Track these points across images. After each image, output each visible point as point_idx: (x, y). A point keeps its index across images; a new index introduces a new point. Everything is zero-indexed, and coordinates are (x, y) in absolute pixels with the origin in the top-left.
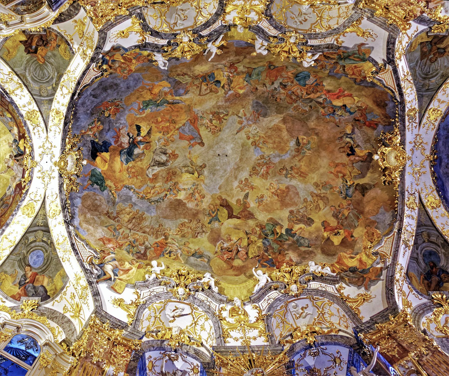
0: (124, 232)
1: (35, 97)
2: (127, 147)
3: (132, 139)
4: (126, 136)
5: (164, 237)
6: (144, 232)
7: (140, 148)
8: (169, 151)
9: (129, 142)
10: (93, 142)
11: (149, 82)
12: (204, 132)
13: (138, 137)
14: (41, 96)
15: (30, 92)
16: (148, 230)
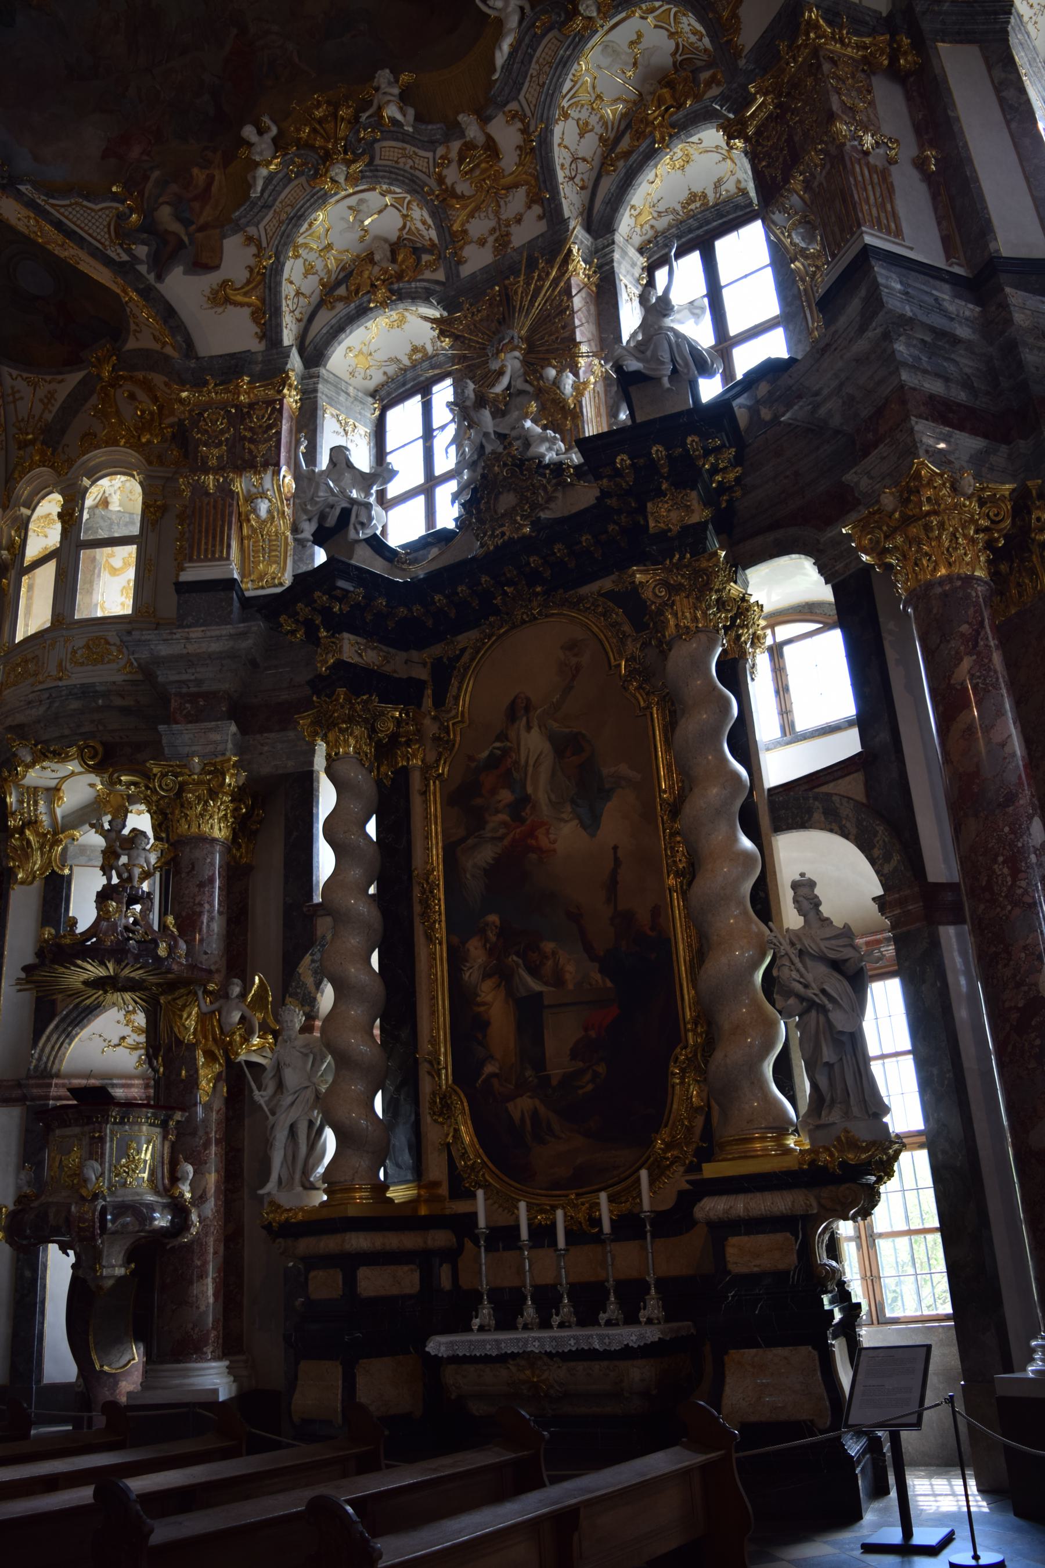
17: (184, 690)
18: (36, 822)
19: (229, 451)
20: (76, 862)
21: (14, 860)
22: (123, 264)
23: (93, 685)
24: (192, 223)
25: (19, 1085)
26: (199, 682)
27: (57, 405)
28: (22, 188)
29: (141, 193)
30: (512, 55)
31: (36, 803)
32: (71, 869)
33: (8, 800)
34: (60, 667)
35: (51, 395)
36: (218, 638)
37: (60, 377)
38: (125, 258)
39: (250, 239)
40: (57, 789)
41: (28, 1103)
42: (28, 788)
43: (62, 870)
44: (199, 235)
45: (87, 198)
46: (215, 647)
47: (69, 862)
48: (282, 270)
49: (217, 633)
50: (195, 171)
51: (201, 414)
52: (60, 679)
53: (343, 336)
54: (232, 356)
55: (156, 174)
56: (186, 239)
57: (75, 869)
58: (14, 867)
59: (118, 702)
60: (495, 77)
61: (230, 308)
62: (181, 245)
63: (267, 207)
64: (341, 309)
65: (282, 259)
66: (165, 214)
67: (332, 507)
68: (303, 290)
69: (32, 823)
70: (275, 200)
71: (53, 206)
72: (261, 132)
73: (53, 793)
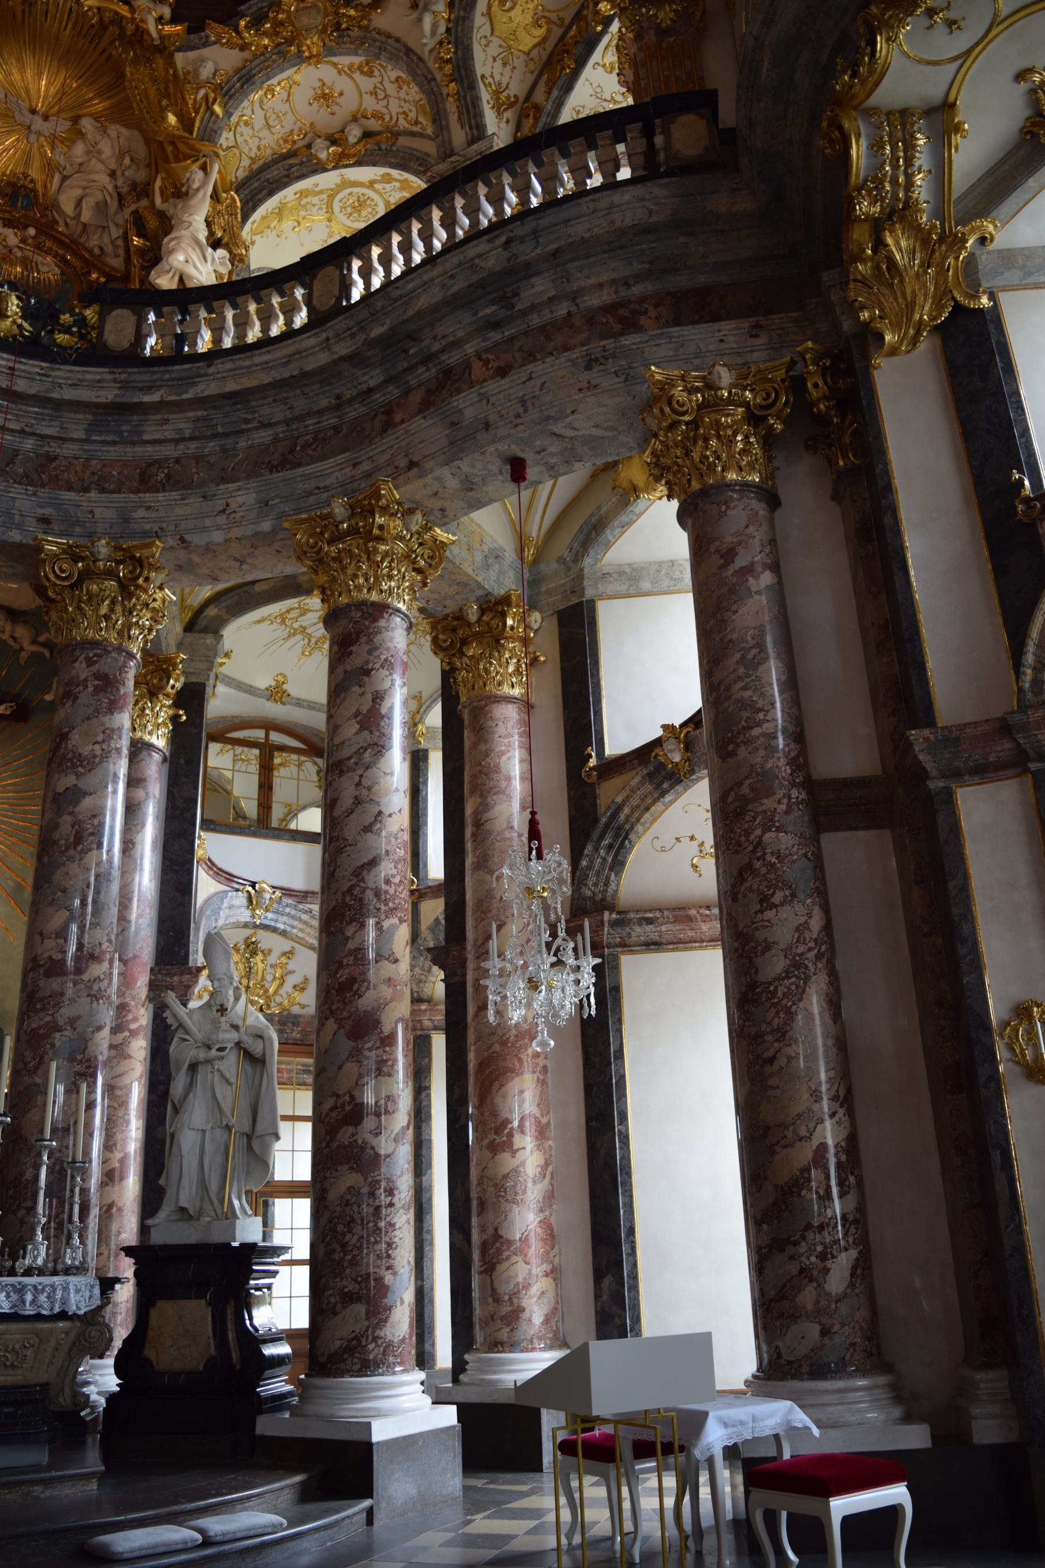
18: (907, 205)
20: (998, 282)
21: (862, 308)
25: (1004, 728)
31: (910, 146)
32: (992, 297)
33: (854, 152)
40: (947, 106)
41: (1033, 766)
42: (888, 114)
43: (976, 297)
47: (985, 284)
57: (1003, 298)
58: (872, 318)
69: (900, 213)
73: (942, 116)
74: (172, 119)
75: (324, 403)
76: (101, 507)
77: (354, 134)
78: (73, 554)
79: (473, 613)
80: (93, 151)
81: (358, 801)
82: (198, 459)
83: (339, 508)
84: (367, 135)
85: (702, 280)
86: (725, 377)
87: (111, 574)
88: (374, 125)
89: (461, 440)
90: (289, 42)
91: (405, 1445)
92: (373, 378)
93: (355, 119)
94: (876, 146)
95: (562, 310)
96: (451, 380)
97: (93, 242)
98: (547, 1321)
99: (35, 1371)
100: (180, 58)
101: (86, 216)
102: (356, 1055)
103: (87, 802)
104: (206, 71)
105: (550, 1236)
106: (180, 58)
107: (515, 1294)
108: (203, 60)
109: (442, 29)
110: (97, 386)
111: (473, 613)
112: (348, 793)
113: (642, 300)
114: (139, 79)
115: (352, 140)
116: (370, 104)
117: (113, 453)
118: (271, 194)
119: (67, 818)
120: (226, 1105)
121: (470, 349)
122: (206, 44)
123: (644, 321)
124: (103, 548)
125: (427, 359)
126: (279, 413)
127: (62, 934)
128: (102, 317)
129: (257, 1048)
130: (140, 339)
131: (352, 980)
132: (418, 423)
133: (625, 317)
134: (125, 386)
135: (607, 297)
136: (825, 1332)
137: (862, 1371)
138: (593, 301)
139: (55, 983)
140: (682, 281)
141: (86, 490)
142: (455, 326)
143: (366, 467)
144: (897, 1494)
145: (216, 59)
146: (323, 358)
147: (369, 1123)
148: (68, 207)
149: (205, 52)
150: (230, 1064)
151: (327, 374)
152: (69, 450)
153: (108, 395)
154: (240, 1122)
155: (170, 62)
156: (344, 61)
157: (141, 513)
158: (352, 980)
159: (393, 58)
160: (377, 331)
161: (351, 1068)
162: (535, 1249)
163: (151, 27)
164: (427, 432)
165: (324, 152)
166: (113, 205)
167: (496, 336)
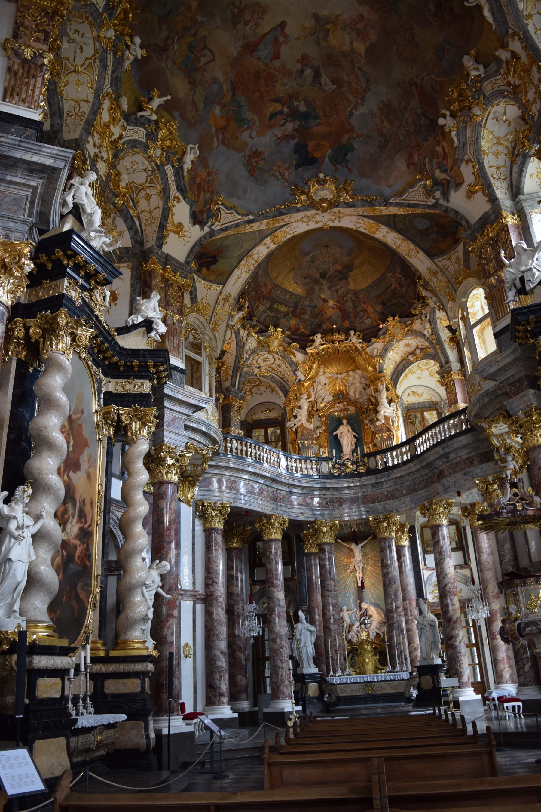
0: (402, 134)
1: (257, 242)
2: (298, 122)
3: (288, 119)
4: (284, 128)
5: (414, 87)
6: (406, 110)
7: (298, 106)
8: (299, 66)
9: (292, 121)
10: (297, 167)
11: (215, 139)
12: (266, 26)
13: (285, 112)
14: (255, 238)
15: (254, 248)
16: (403, 103)
17: (510, 382)
19: (496, 262)
22: (434, 204)
23: (488, 390)
24: (447, 170)
26: (513, 376)
27: (462, 260)
28: (391, 201)
29: (427, 171)
30: (493, 14)
34: (480, 385)
35: (457, 258)
36: (508, 356)
37: (456, 250)
38: (434, 201)
39: (467, 162)
44: (452, 173)
45: (411, 188)
46: (509, 360)
48: (484, 166)
49: (506, 354)
50: (437, 148)
51: (481, 252)
52: (480, 390)
53: (524, 173)
54: (480, 219)
55: (427, 160)
56: (448, 178)
59: (500, 392)
60: (494, 27)
61: (475, 195)
62: (448, 182)
63: (465, 144)
64: (519, 160)
65: (481, 161)
66: (438, 173)
67: (515, 279)
68: (499, 165)
70: (466, 139)
71: (403, 200)
72: (445, 117)
74: (370, 368)
75: (419, 475)
76: (379, 506)
77: (418, 352)
78: (375, 519)
79: (469, 507)
80: (354, 378)
81: (441, 572)
82: (396, 489)
83: (426, 502)
84: (422, 349)
85: (485, 450)
86: (490, 478)
87: (384, 521)
88: (422, 347)
89: (446, 490)
90: (394, 338)
91: (467, 702)
92: (427, 471)
93: (417, 348)
94: (499, 442)
95: (458, 459)
96: (441, 475)
97: (361, 401)
98: (510, 677)
99: (401, 690)
100: (368, 350)
101: (357, 396)
102: (449, 626)
103: (390, 575)
104: (375, 353)
105: (509, 658)
106: (368, 350)
107: (501, 671)
108: (373, 349)
109: (430, 331)
110: (371, 480)
111: (469, 507)
112: (439, 570)
113: (473, 456)
114: (360, 360)
115: (418, 353)
116: (419, 344)
117: (378, 492)
118: (401, 374)
119: (387, 579)
120: (428, 636)
121: (444, 466)
122: (373, 344)
123: (475, 462)
124: (381, 517)
125: (436, 468)
126: (410, 479)
127: (391, 604)
128: (368, 460)
129: (433, 624)
130: (377, 464)
131: (446, 611)
132: (436, 484)
133: (470, 462)
134: (377, 478)
135: (466, 456)
136: (525, 678)
137: (535, 685)
138: (464, 457)
139: (392, 614)
140: (481, 451)
141: (374, 502)
142: (439, 463)
143: (429, 493)
144: (520, 703)
145: (377, 345)
146: (415, 469)
147: (454, 639)
148: (351, 394)
149: (375, 346)
150: (428, 628)
151: (418, 471)
152: (369, 493)
153: (374, 481)
154: (432, 639)
155: (366, 353)
156: (410, 338)
157: (387, 506)
158: (446, 611)
159: (421, 337)
160: (424, 464)
161: (448, 629)
162: (506, 661)
163: (359, 347)
164: (438, 486)
165: (412, 358)
166: (363, 391)
167: (447, 464)
